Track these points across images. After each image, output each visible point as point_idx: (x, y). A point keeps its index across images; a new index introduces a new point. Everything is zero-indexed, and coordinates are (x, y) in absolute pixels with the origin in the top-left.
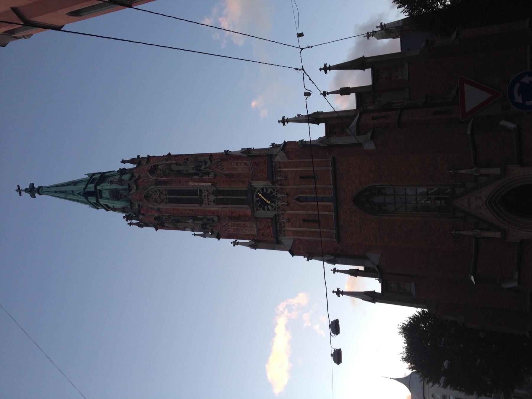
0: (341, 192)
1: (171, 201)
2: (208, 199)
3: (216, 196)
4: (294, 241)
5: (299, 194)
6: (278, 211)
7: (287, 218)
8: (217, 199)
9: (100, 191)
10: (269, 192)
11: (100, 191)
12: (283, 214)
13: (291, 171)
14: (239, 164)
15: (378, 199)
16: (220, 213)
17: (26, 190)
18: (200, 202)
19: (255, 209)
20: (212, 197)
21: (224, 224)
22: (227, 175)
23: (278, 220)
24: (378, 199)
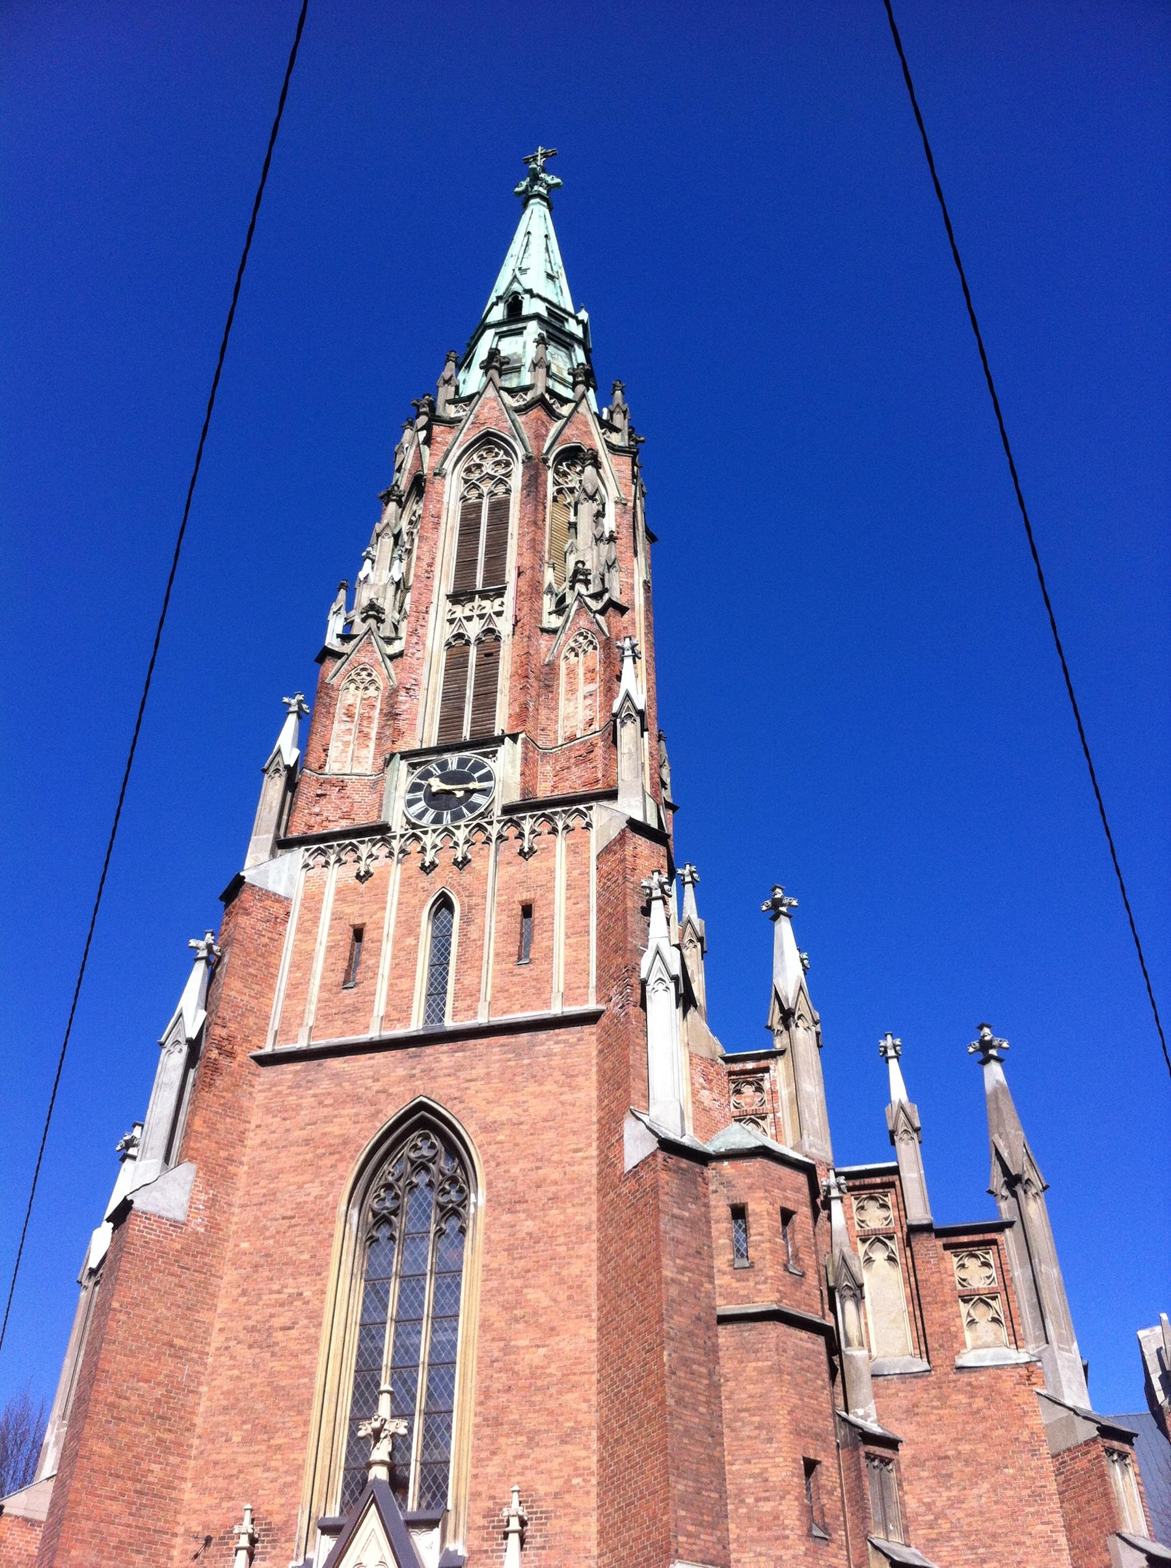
0: (460, 1054)
2: (469, 619)
3: (479, 641)
5: (462, 905)
6: (402, 836)
7: (372, 870)
8: (468, 643)
12: (391, 854)
13: (552, 871)
14: (589, 701)
16: (413, 654)
19: (416, 760)
20: (473, 629)
21: (374, 673)
23: (366, 839)
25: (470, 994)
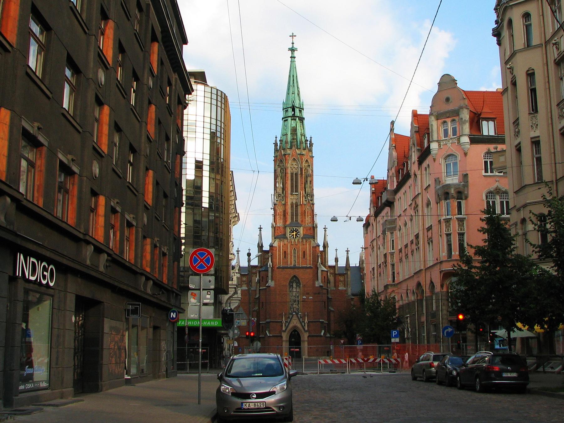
1: (292, 174)
4: (276, 247)
9: (295, 120)
10: (298, 235)
11: (295, 120)
12: (288, 241)
15: (294, 285)
17: (293, 43)
18: (291, 194)
20: (294, 202)
22: (305, 211)
24: (294, 285)
25: (299, 262)
